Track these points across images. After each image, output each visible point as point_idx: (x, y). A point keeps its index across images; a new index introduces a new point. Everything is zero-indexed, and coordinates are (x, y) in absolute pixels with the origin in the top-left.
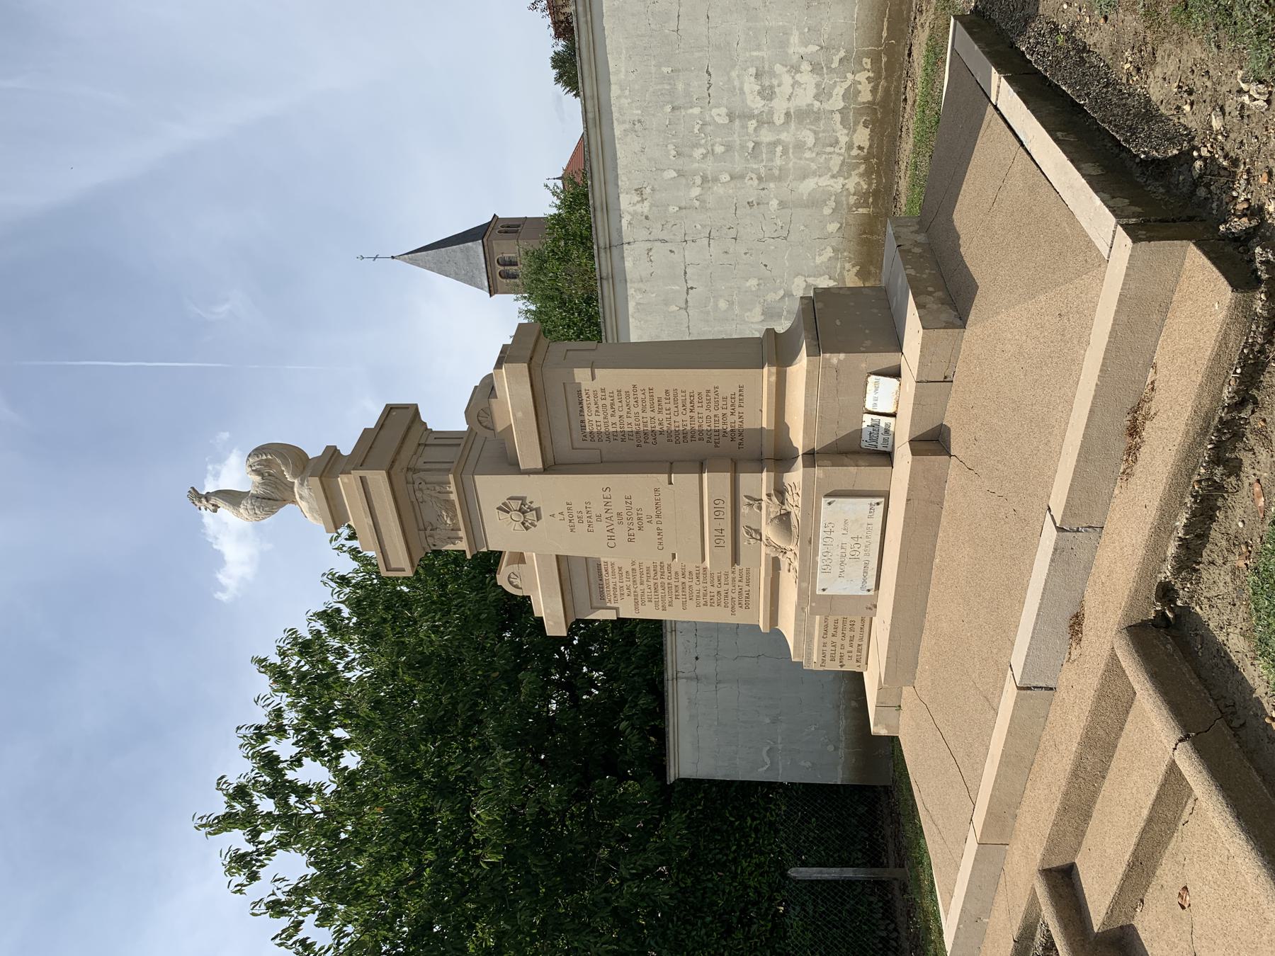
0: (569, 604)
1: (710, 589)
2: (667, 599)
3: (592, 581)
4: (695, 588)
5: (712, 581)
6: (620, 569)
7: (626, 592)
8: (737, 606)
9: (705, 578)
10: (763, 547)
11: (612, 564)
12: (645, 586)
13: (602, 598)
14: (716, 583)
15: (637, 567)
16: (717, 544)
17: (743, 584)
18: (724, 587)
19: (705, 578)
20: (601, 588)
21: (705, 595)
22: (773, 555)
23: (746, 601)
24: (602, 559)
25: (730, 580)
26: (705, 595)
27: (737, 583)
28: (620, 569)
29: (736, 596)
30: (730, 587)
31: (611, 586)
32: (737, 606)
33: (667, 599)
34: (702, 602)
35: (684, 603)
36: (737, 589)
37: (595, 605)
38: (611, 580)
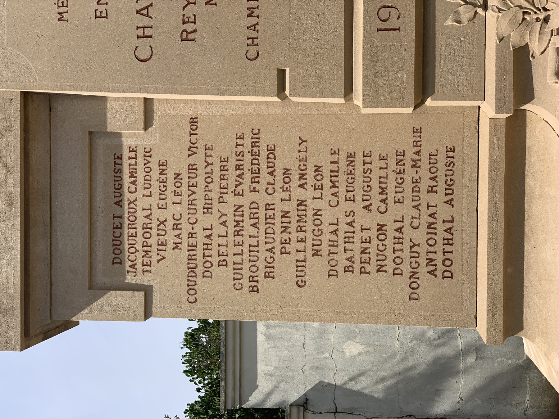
0: (39, 268)
1: (363, 219)
2: (263, 254)
3: (99, 203)
4: (328, 215)
5: (367, 196)
6: (163, 166)
7: (170, 238)
8: (423, 270)
9: (350, 184)
10: (491, 16)
11: (147, 154)
12: (212, 219)
13: (118, 260)
14: (375, 202)
15: (199, 159)
16: (382, 26)
17: (438, 199)
18: (395, 211)
19: (350, 184)
20: (117, 240)
21: (349, 240)
22: (515, 39)
23: (443, 259)
24: (127, 142)
25: (408, 185)
26: (349, 240)
27: (425, 197)
28: (163, 166)
29: (420, 236)
30: (407, 210)
31: (141, 221)
32: (423, 270)
33: (263, 254)
34: (341, 258)
35: (301, 265)
36: (425, 219)
37: (100, 279)
38: (141, 200)
